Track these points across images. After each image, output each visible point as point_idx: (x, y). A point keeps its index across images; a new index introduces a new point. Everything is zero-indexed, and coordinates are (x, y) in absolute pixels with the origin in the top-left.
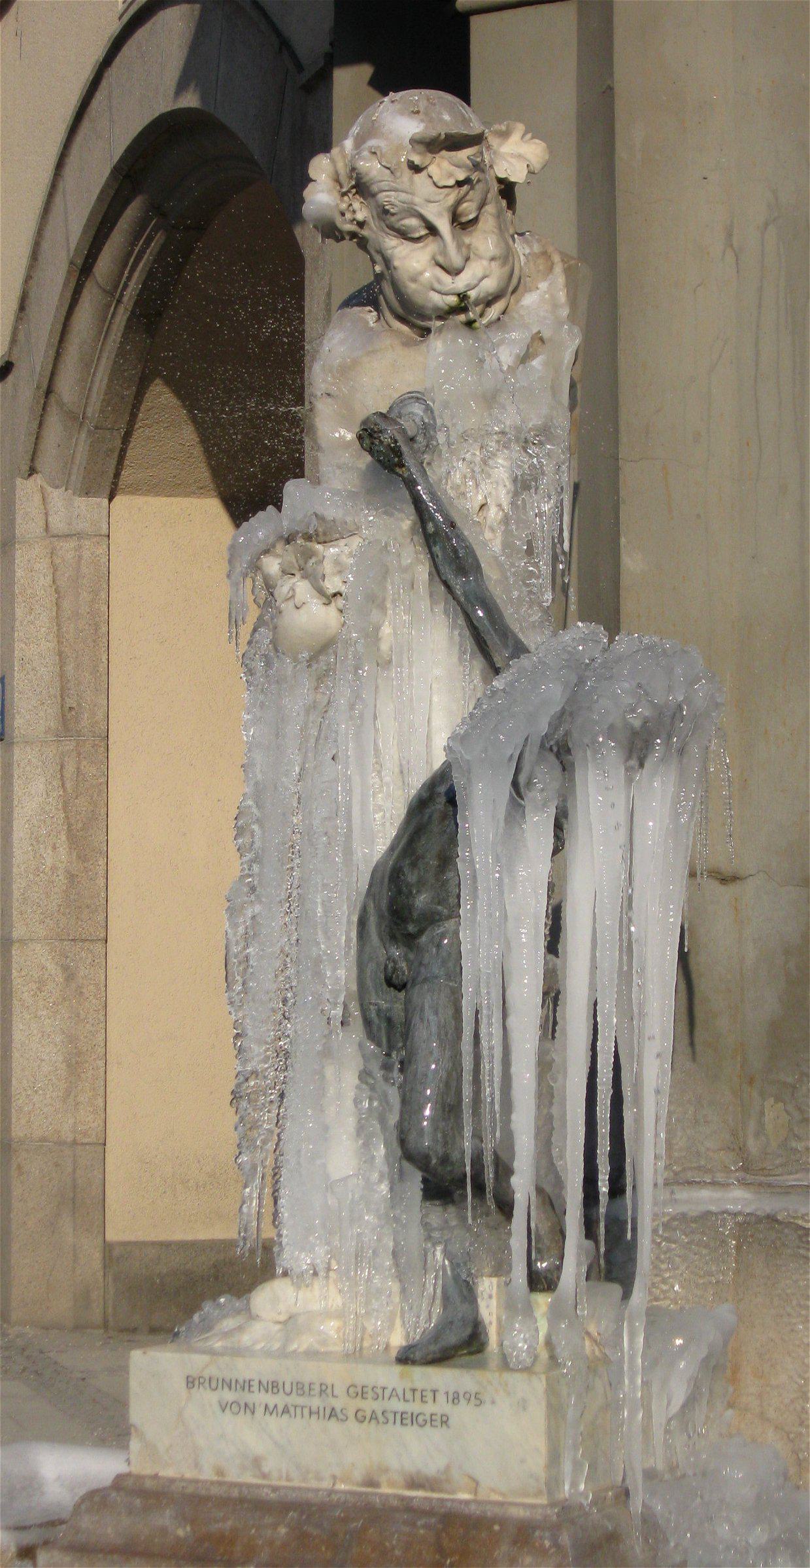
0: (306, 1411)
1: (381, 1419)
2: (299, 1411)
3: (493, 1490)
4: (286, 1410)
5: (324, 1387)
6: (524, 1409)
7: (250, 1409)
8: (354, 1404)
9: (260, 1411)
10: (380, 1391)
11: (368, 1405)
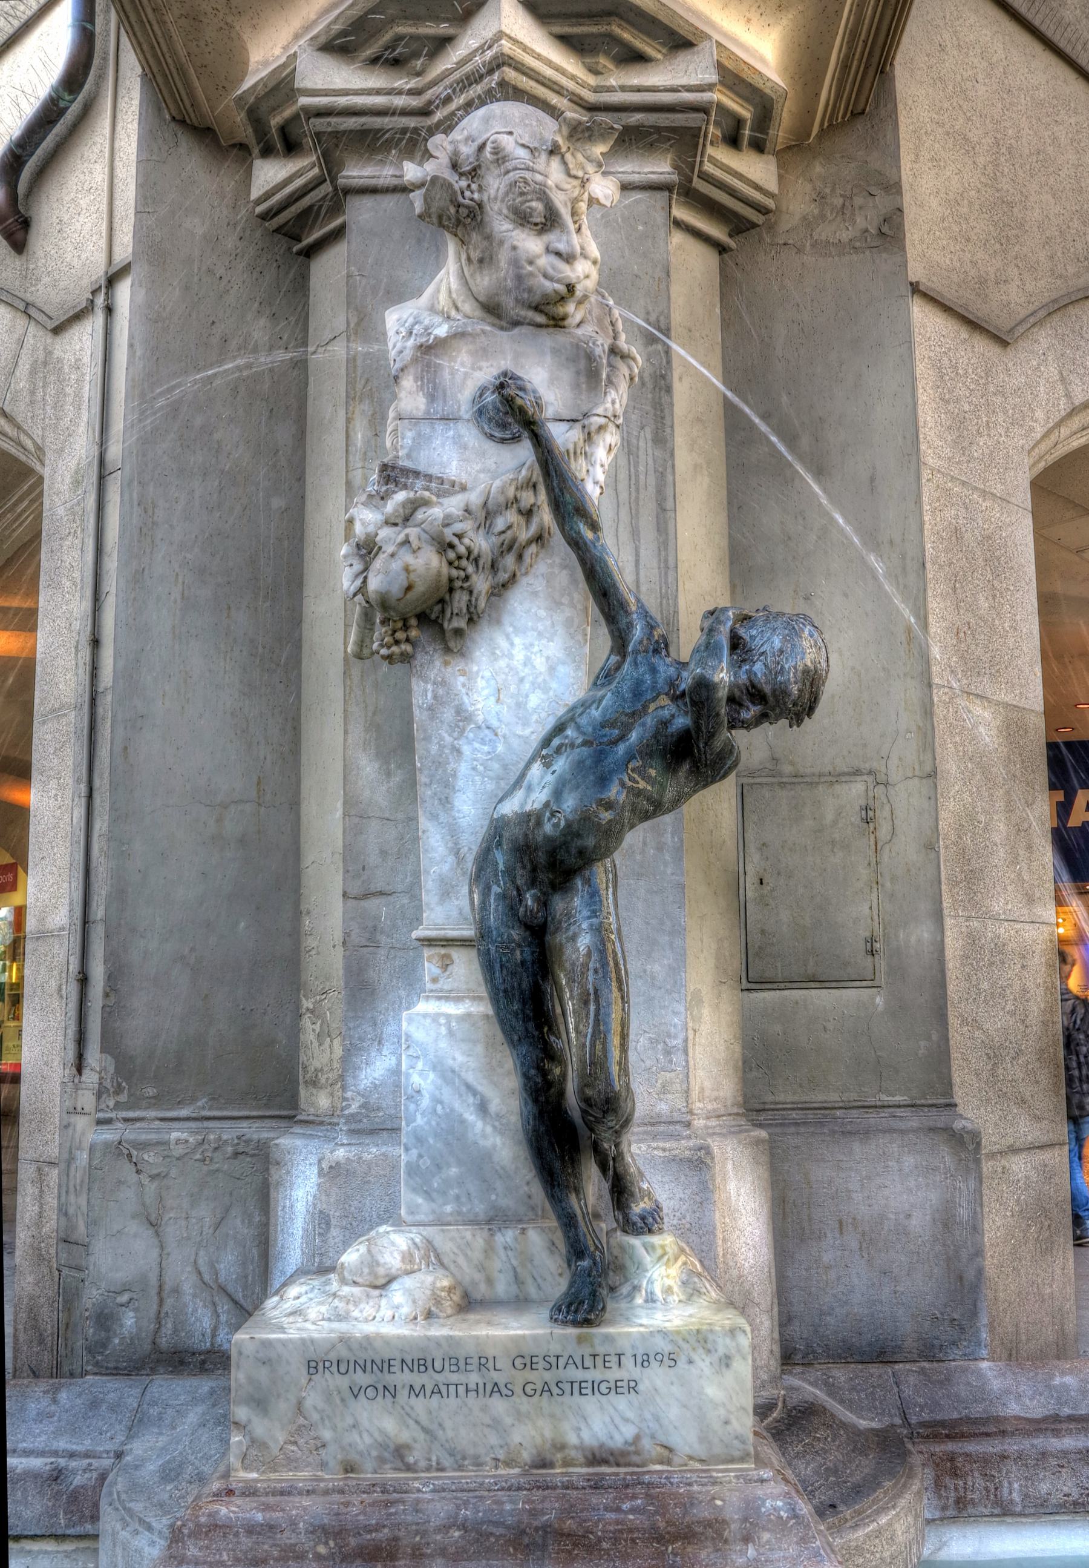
0: (461, 1389)
1: (555, 1390)
2: (452, 1389)
3: (691, 1458)
4: (437, 1391)
5: (483, 1361)
6: (727, 1366)
7: (391, 1391)
8: (521, 1377)
10: (553, 1360)
11: (537, 1377)
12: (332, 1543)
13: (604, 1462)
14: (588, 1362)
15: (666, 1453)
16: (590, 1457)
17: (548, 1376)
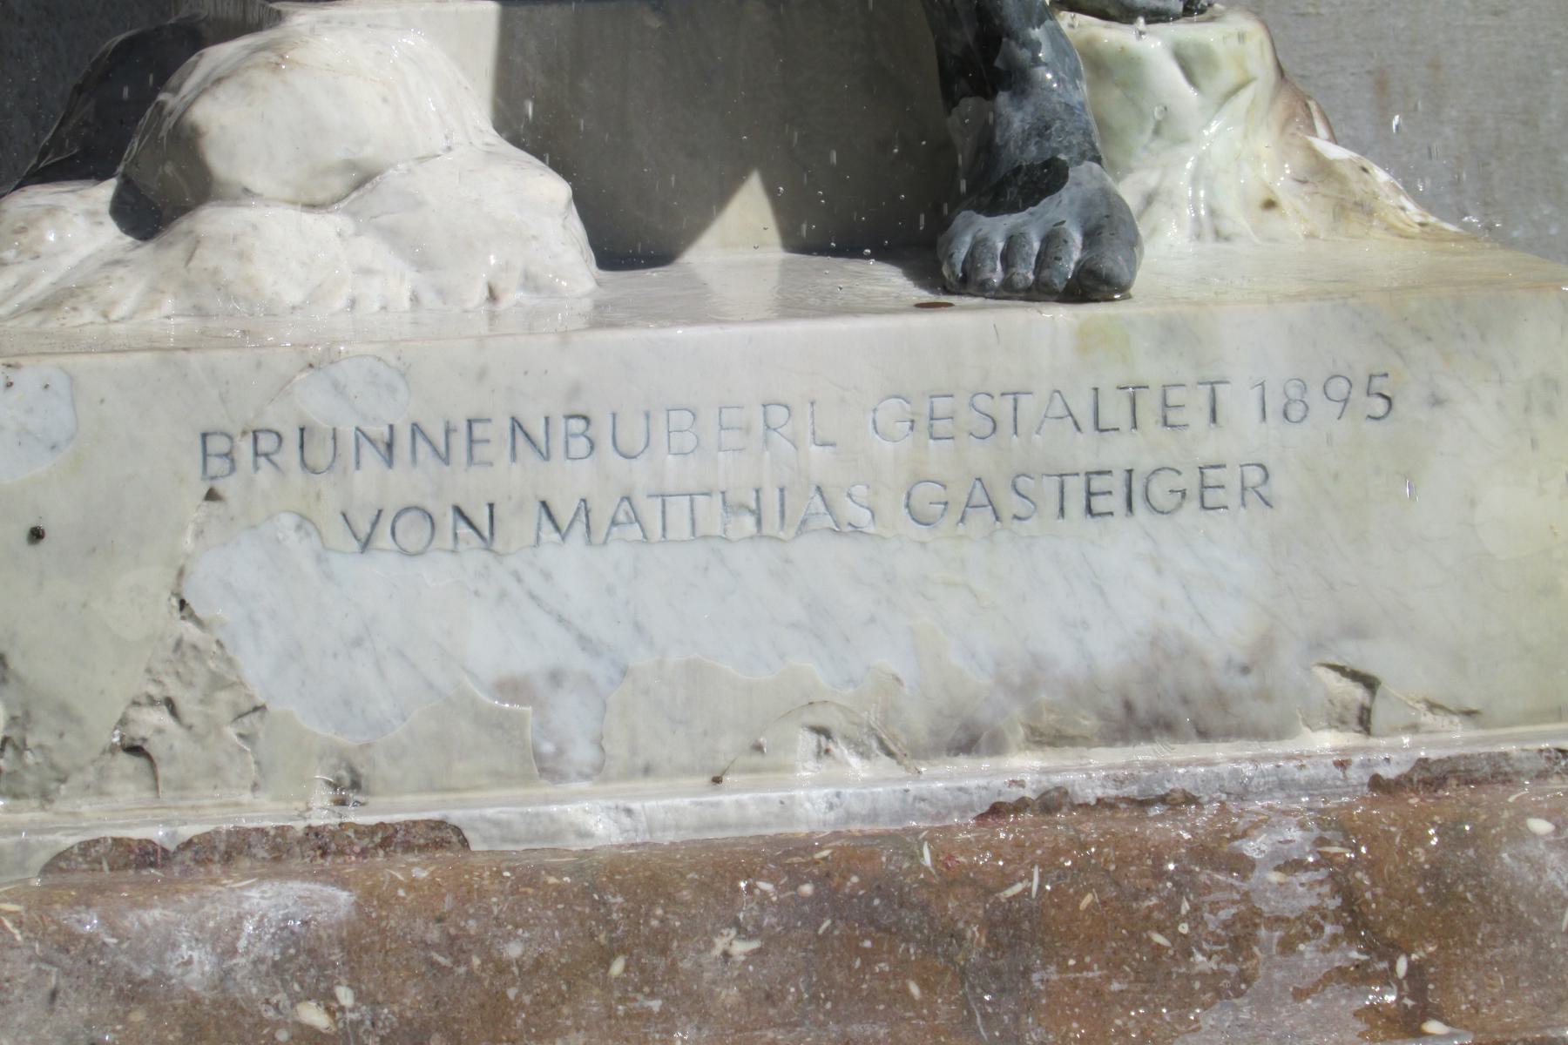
1: (1010, 504)
7: (477, 525)
9: (518, 527)
10: (1003, 408)
12: (345, 996)
13: (1159, 726)
14: (1115, 412)
15: (1358, 693)
16: (1118, 712)
17: (981, 457)
